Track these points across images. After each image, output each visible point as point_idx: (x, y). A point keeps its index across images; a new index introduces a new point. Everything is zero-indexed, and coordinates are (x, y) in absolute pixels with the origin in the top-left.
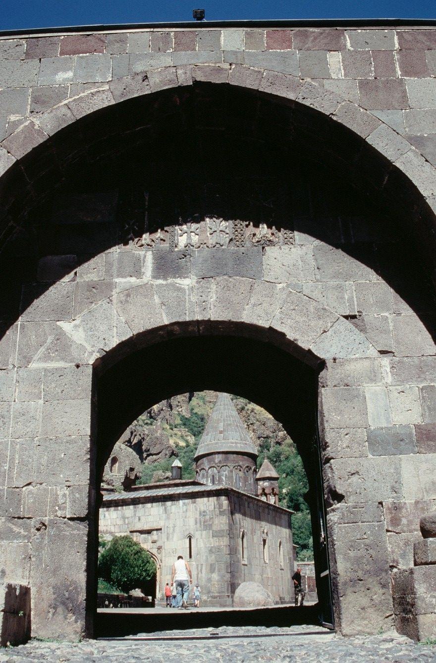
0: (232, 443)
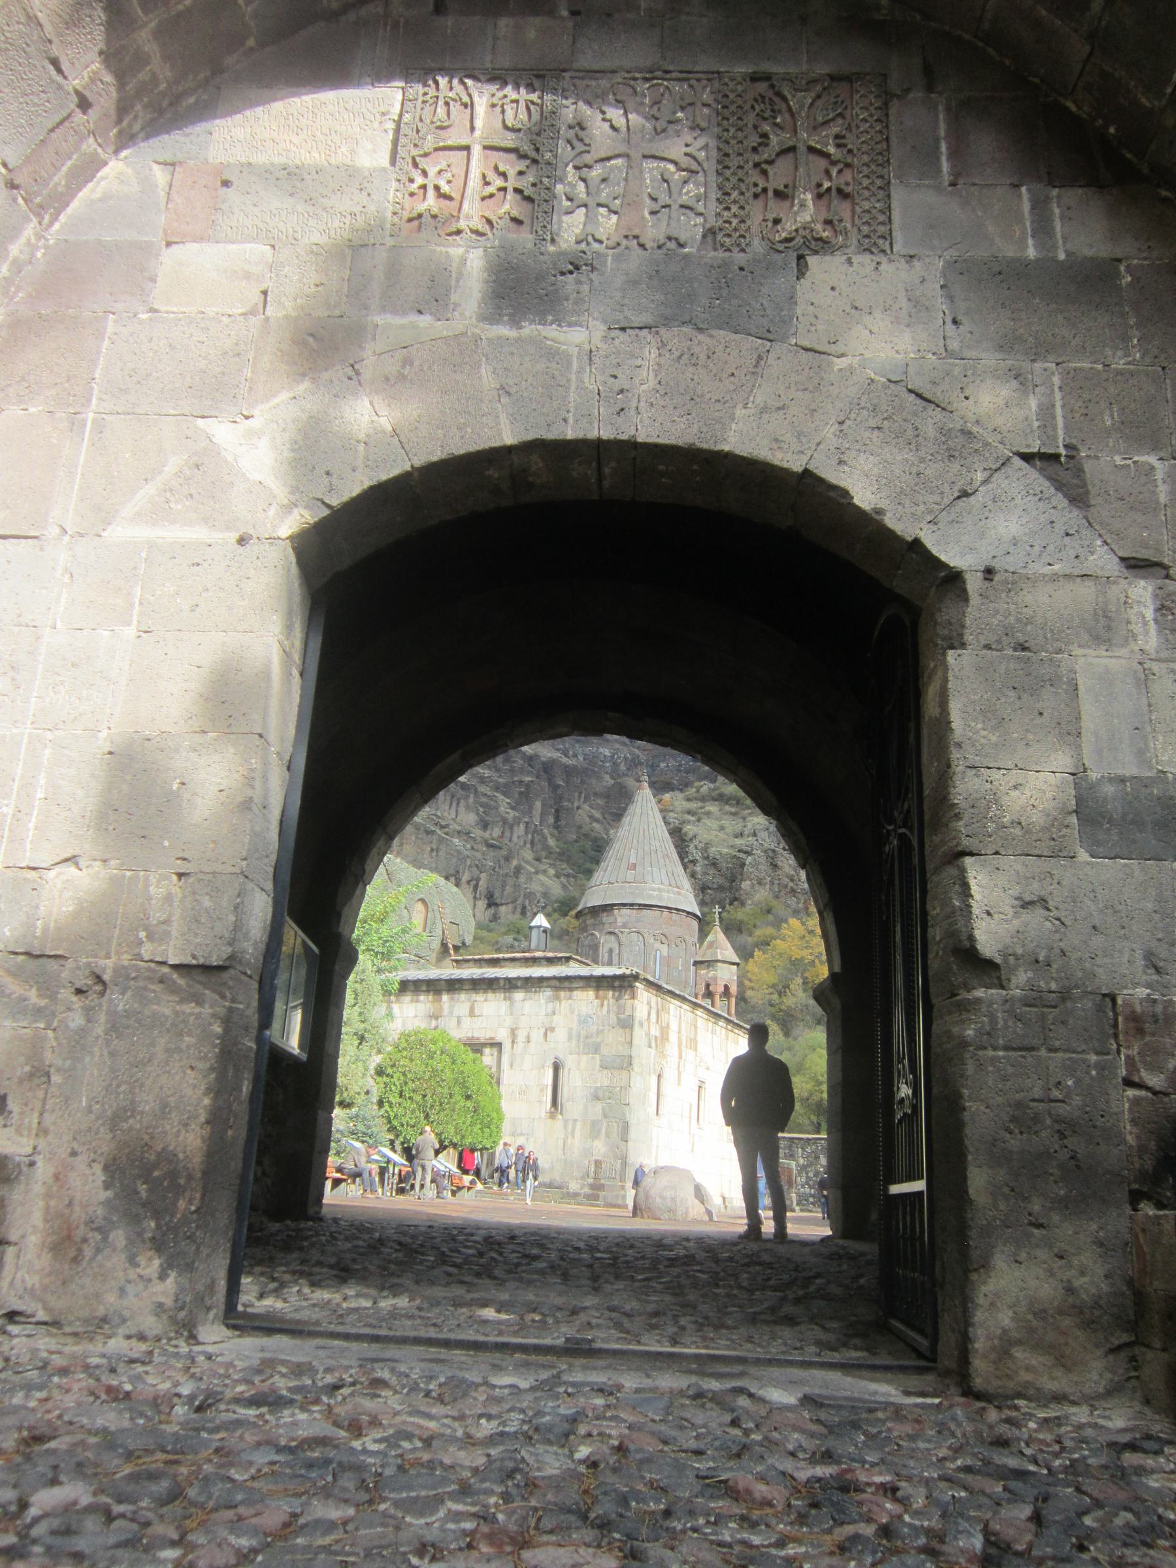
0: (653, 890)
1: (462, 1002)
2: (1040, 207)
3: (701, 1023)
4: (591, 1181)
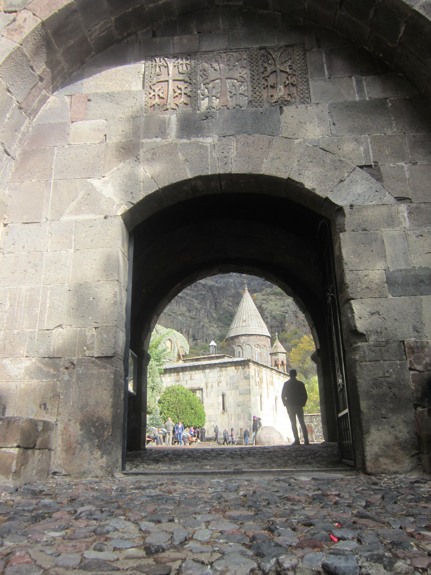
0: (253, 329)
1: (187, 375)
2: (359, 83)
3: (274, 375)
4: (239, 436)
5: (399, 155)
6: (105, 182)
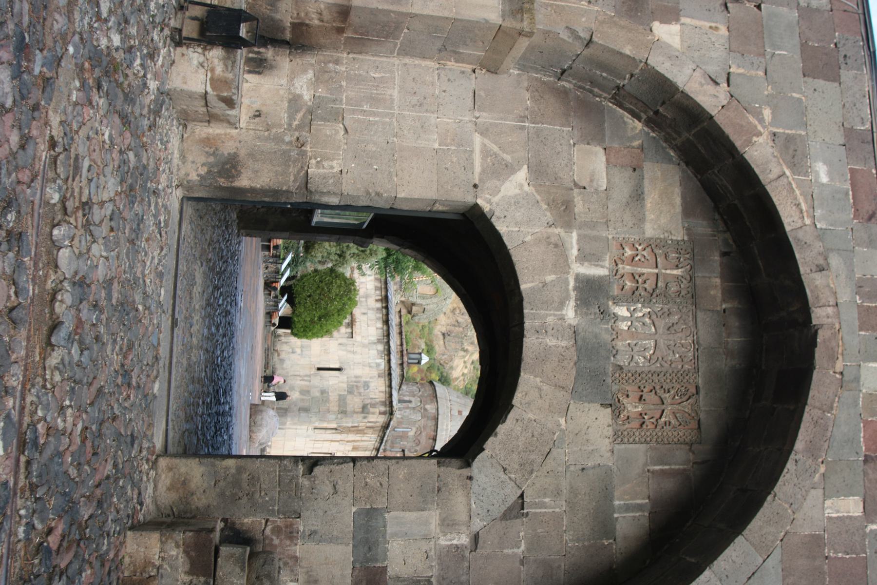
0: (447, 426)
2: (640, 507)
5: (534, 543)
6: (521, 186)
